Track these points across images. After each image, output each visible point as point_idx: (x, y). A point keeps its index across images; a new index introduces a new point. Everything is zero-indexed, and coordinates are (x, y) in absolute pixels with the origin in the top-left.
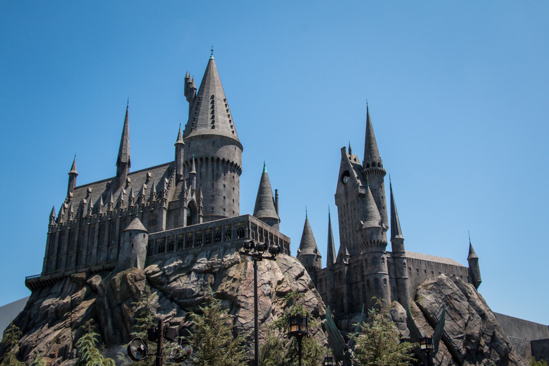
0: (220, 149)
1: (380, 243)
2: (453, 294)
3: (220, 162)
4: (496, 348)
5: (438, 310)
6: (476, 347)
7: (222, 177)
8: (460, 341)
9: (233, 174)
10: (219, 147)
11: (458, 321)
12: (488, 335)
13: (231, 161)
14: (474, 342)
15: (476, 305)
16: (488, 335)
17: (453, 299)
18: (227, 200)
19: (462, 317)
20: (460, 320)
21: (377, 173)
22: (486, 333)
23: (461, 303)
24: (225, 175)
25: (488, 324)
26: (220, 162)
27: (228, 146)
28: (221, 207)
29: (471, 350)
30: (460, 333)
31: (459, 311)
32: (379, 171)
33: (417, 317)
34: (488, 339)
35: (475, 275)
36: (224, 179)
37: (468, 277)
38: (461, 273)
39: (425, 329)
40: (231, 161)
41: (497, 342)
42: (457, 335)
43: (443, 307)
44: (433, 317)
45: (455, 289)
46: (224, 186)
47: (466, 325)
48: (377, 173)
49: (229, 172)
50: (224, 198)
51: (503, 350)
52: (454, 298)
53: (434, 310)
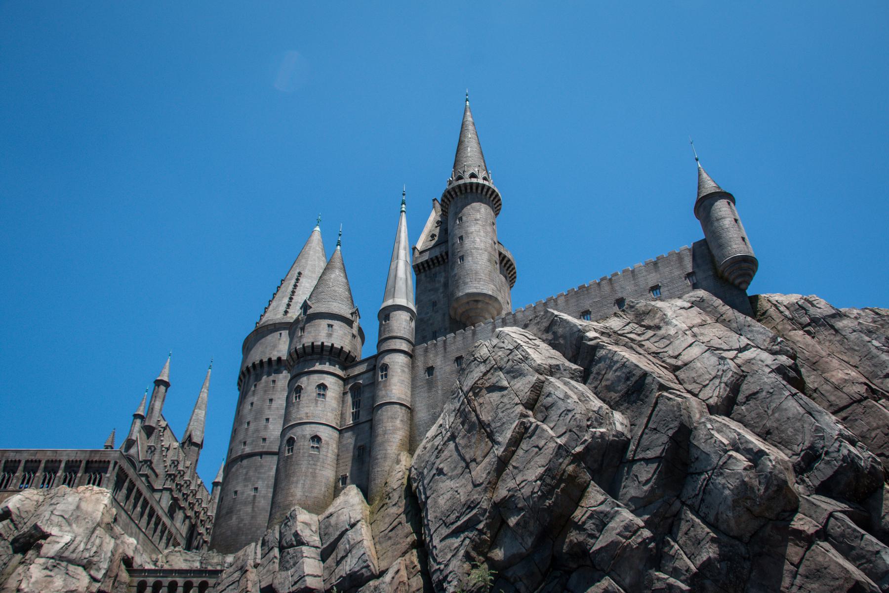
0: (252, 352)
1: (295, 356)
2: (489, 375)
3: (252, 370)
4: (703, 500)
5: (433, 458)
6: (530, 541)
7: (250, 393)
8: (456, 542)
9: (271, 378)
10: (251, 350)
11: (478, 464)
12: (648, 461)
13: (265, 360)
14: (517, 524)
15: (617, 362)
16: (648, 461)
17: (484, 391)
18: (252, 427)
19: (494, 442)
20: (485, 457)
21: (451, 199)
22: (641, 456)
23: (505, 392)
24: (255, 386)
25: (657, 409)
26: (252, 370)
27: (263, 340)
28: (240, 442)
29: (510, 562)
30: (469, 507)
31: (489, 425)
32: (453, 193)
33: (385, 508)
34: (643, 478)
35: (715, 252)
36: (254, 395)
37: (689, 276)
38: (653, 279)
39: (390, 538)
40: (265, 360)
41: (700, 474)
42: (458, 518)
43: (453, 438)
44: (417, 487)
45: (500, 353)
46: (252, 404)
47: (502, 464)
48: (451, 199)
49: (265, 377)
50: (248, 423)
51: (730, 501)
52: (487, 388)
53: (423, 462)
